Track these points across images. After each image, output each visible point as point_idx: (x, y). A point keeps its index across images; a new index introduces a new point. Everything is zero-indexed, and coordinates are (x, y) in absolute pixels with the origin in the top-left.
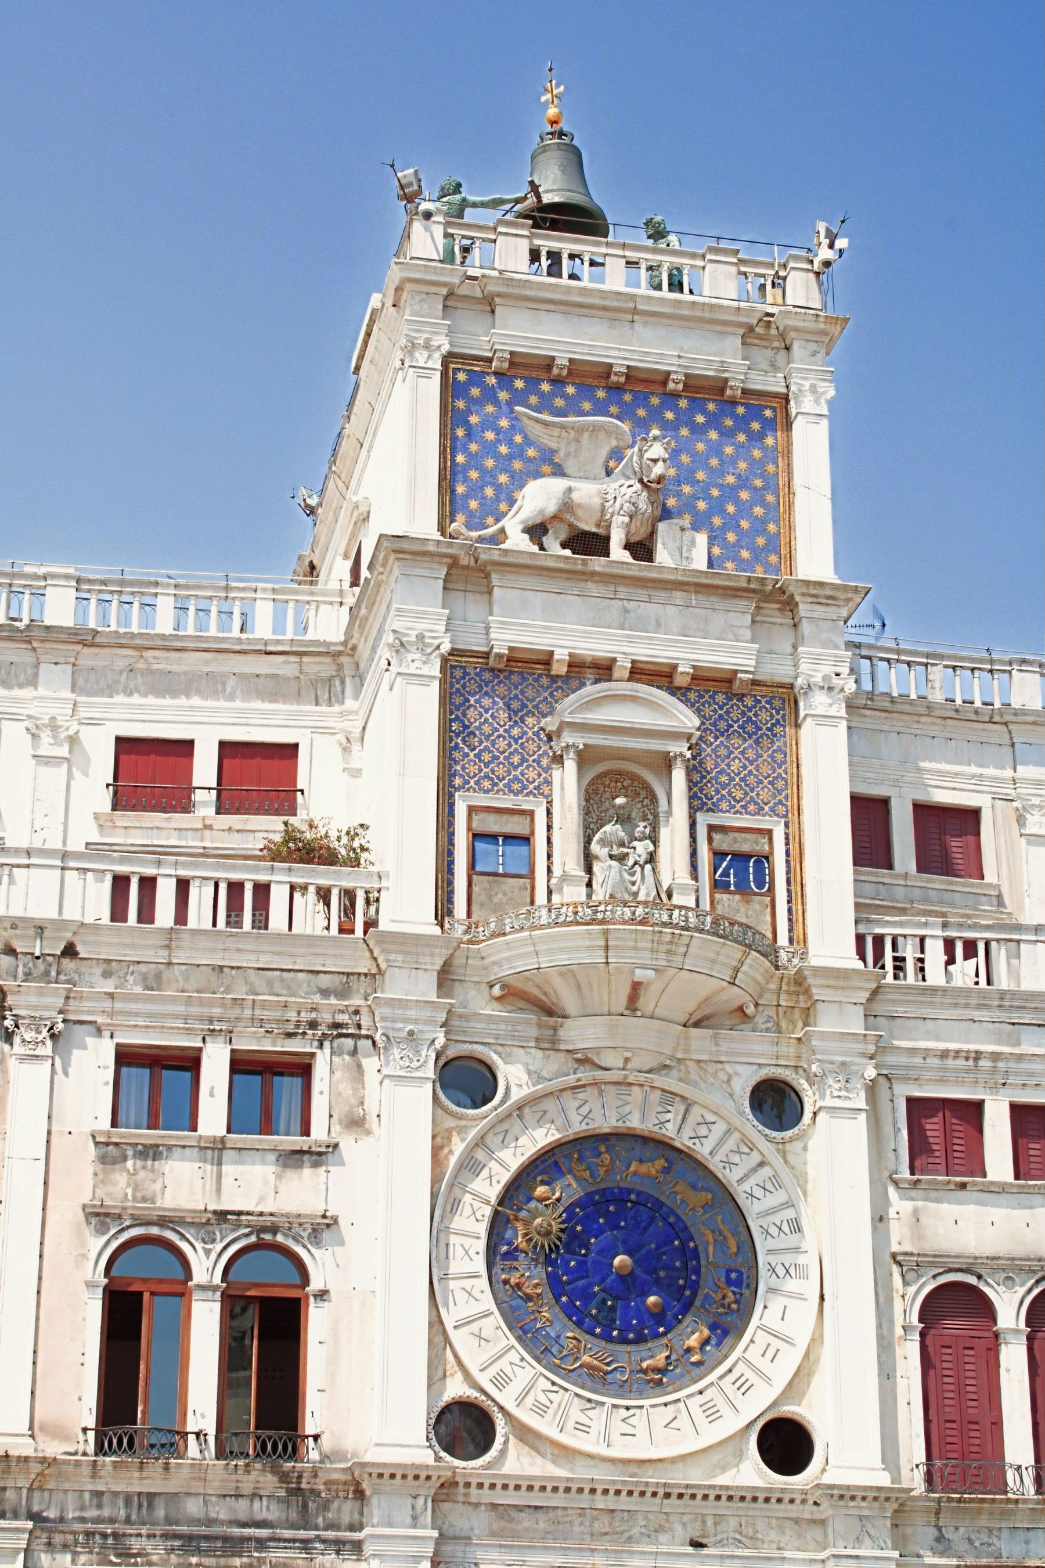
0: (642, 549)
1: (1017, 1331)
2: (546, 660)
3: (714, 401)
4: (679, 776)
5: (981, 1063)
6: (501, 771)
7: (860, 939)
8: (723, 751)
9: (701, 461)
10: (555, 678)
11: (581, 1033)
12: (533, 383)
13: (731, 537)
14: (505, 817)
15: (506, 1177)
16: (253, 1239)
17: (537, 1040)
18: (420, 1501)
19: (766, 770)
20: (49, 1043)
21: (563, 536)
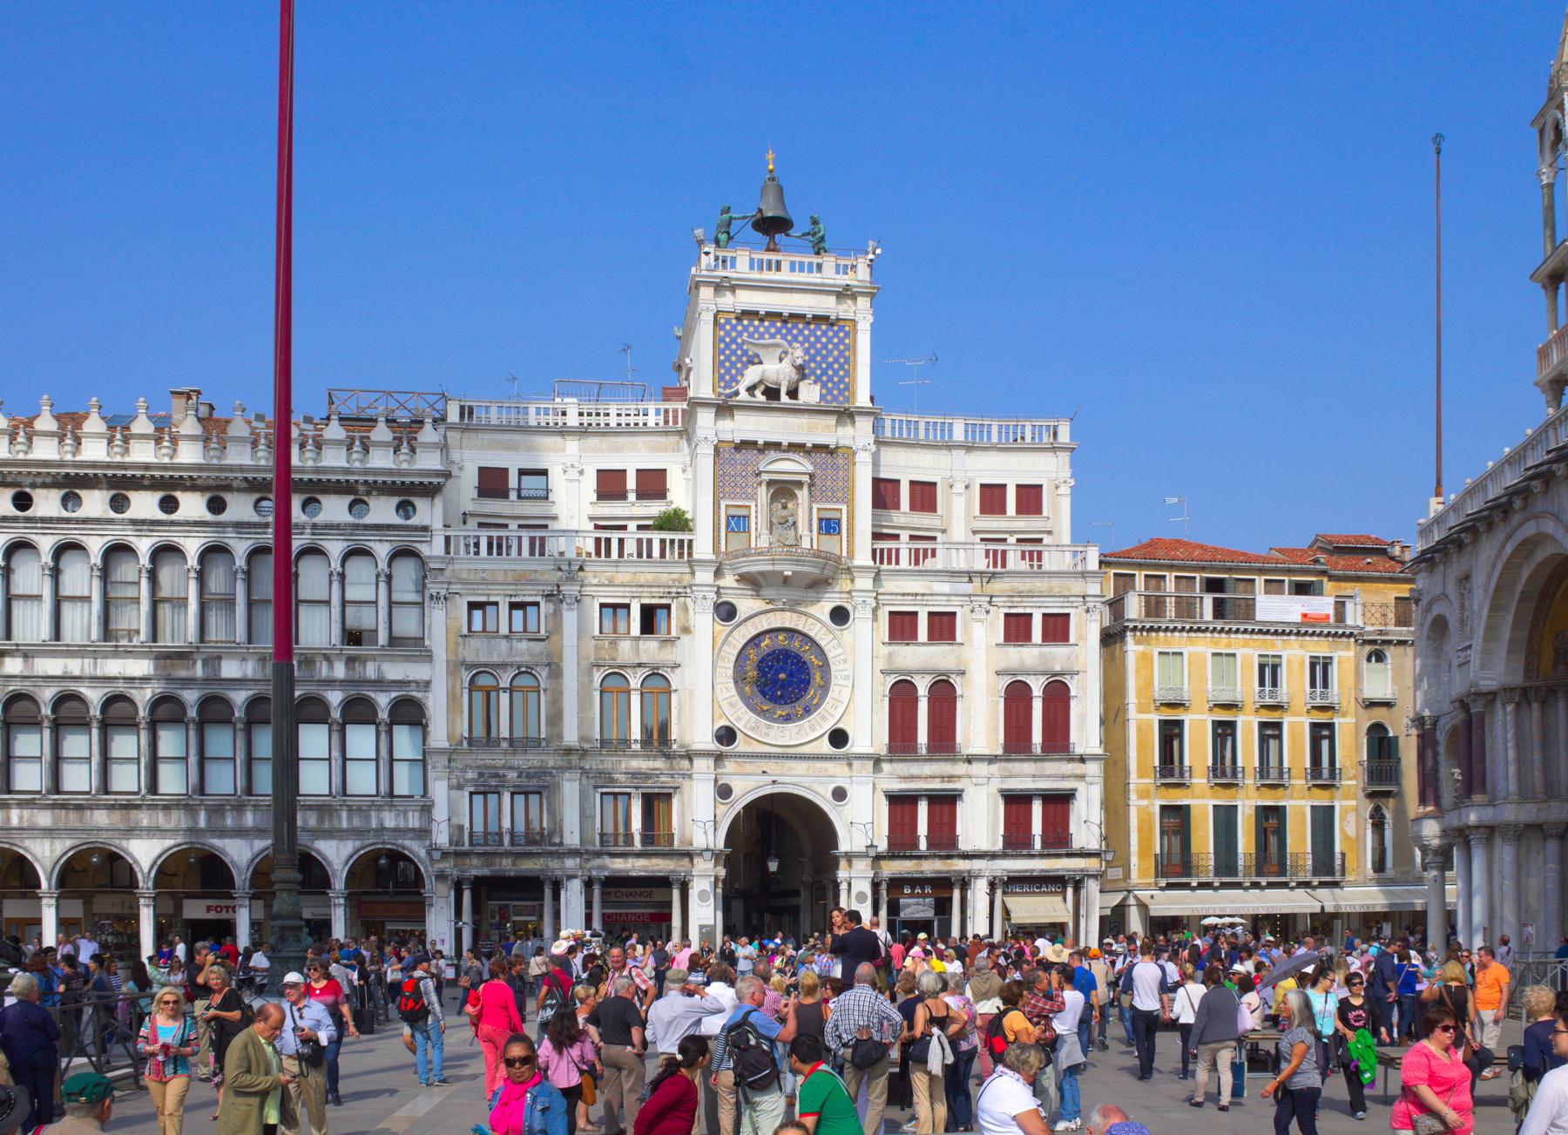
0: (793, 393)
2: (755, 443)
4: (806, 489)
7: (874, 551)
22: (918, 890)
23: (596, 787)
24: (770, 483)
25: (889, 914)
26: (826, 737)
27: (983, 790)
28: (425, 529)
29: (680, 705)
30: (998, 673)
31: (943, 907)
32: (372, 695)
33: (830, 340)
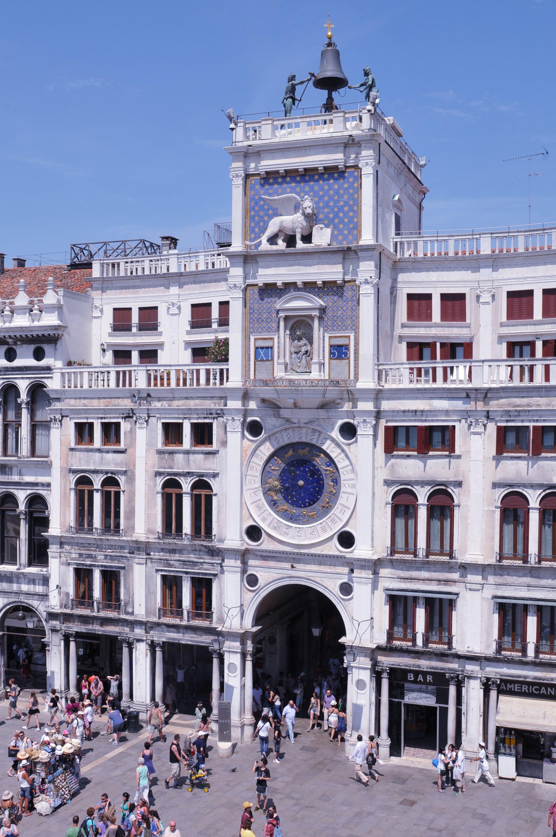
0: (307, 238)
1: (423, 505)
3: (337, 173)
4: (316, 323)
5: (417, 413)
6: (264, 325)
8: (335, 309)
9: (331, 198)
10: (281, 290)
11: (285, 413)
12: (275, 179)
13: (341, 226)
14: (265, 341)
15: (265, 458)
16: (197, 479)
17: (274, 415)
18: (237, 556)
19: (349, 313)
20: (145, 423)
21: (282, 238)
22: (420, 678)
23: (157, 571)
24: (286, 318)
25: (391, 695)
26: (336, 538)
27: (477, 594)
28: (48, 369)
29: (219, 506)
30: (495, 485)
31: (443, 697)
32: (15, 492)
33: (341, 187)
